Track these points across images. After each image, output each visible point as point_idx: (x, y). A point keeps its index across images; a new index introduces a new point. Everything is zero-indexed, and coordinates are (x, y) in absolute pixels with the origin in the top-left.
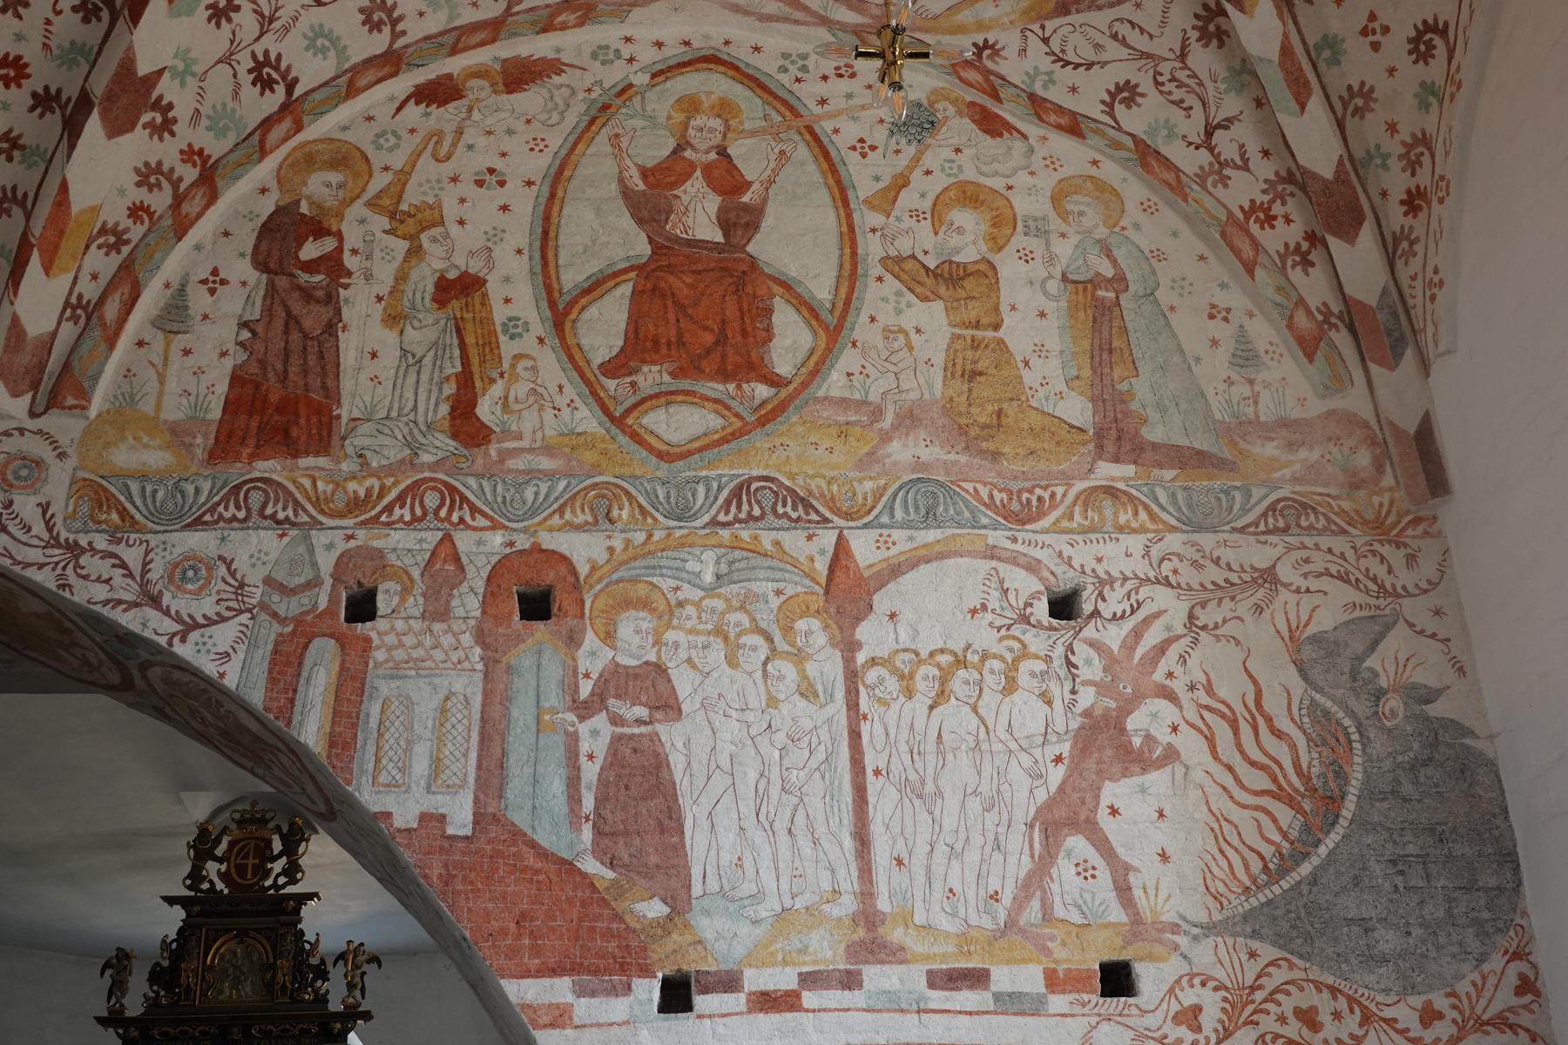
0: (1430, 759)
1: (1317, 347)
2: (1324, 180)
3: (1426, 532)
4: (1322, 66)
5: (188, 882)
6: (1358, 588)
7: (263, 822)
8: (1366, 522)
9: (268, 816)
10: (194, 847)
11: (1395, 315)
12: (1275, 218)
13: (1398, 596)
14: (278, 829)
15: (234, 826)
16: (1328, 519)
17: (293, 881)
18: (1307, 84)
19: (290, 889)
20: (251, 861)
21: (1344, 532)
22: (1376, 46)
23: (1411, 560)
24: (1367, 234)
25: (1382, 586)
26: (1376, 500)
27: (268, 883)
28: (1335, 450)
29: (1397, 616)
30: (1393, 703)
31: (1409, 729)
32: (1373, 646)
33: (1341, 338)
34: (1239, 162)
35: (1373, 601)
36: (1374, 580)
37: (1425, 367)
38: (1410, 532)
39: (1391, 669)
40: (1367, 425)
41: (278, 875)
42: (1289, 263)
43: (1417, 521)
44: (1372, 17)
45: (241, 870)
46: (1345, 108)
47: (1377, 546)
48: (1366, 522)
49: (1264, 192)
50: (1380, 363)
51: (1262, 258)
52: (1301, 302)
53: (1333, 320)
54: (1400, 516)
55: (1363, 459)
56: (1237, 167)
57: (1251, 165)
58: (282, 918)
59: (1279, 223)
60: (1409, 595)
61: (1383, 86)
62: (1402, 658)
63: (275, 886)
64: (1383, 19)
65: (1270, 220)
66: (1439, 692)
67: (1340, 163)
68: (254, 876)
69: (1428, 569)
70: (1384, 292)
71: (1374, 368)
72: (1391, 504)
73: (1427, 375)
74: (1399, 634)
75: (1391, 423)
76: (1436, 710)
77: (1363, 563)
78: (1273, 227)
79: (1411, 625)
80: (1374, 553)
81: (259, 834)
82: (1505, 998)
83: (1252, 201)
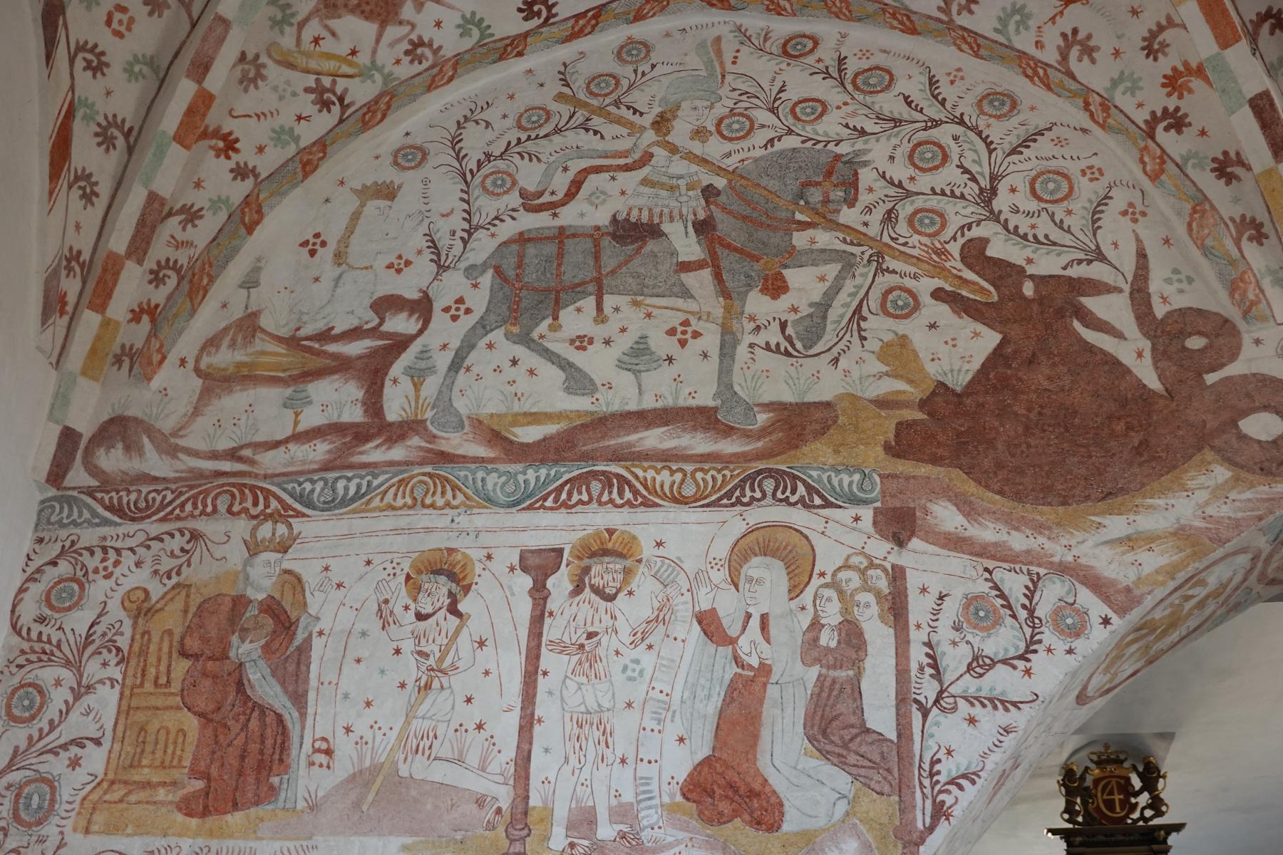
5: (1066, 816)
7: (1119, 762)
9: (1122, 757)
10: (1064, 785)
14: (1135, 768)
15: (1092, 766)
17: (1159, 814)
19: (1157, 821)
20: (1117, 797)
27: (1136, 815)
41: (1143, 809)
45: (1110, 804)
58: (1155, 847)
63: (1142, 817)
68: (1122, 809)
81: (1117, 773)
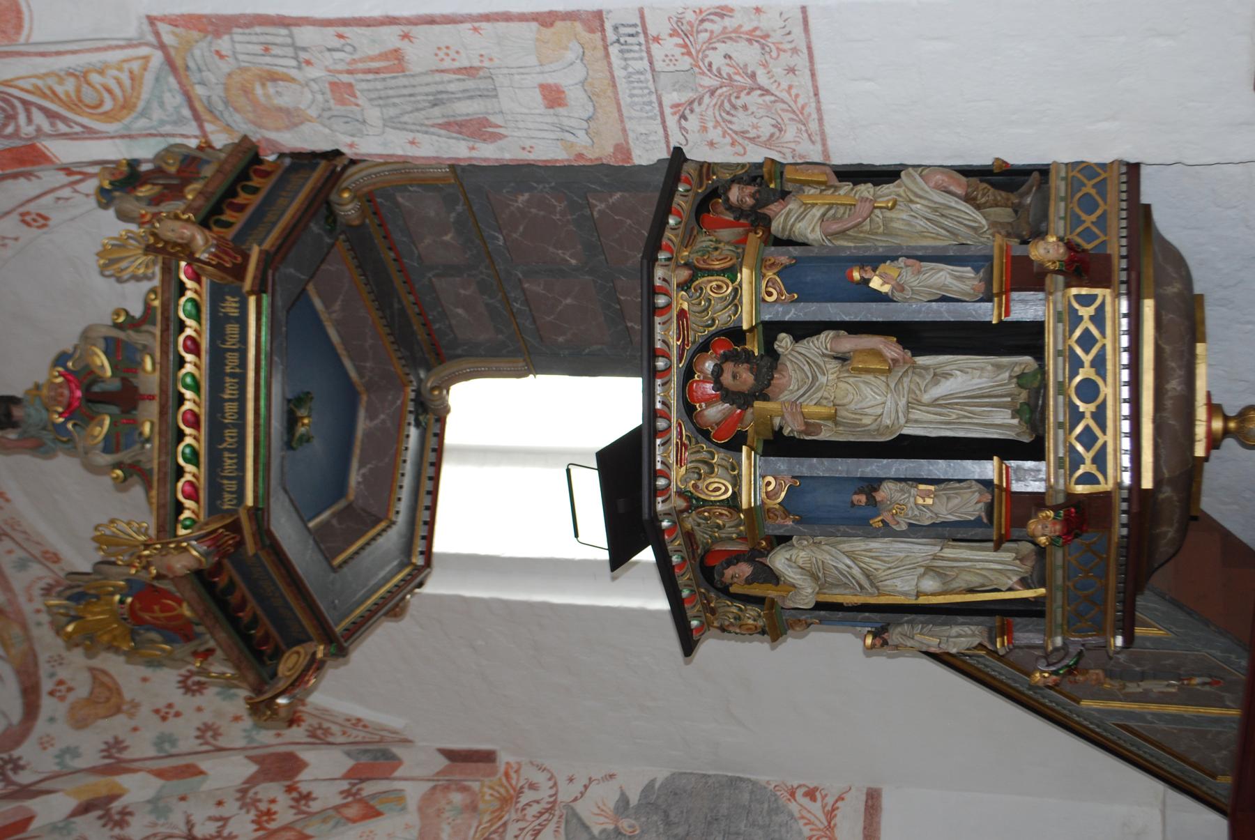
0: (665, 812)
1: (372, 808)
2: (257, 772)
3: (516, 772)
4: (174, 751)
6: (545, 826)
8: (501, 809)
11: (366, 751)
12: (269, 810)
13: (555, 802)
16: (495, 832)
18: (188, 766)
21: (505, 824)
22: (177, 714)
23: (532, 786)
24: (306, 755)
25: (547, 810)
26: (487, 797)
28: (446, 815)
29: (567, 806)
30: (625, 824)
31: (643, 819)
32: (586, 828)
33: (369, 789)
34: (220, 824)
35: (555, 819)
36: (541, 814)
37: (406, 742)
38: (514, 782)
39: (602, 819)
40: (434, 788)
42: (304, 808)
43: (507, 775)
44: (157, 711)
46: (207, 743)
47: (520, 806)
48: (501, 809)
49: (248, 812)
50: (395, 768)
51: (298, 826)
52: (337, 808)
53: (354, 790)
54: (502, 785)
55: (457, 798)
56: (223, 826)
57: (226, 815)
59: (274, 808)
60: (555, 794)
61: (207, 717)
62: (597, 811)
64: (161, 704)
65: (269, 813)
66: (623, 794)
67: (250, 758)
69: (540, 778)
70: (348, 754)
71: (397, 774)
72: (491, 788)
73: (410, 741)
74: (579, 807)
75: (438, 774)
76: (634, 799)
77: (529, 818)
78: (275, 813)
79: (576, 799)
80: (523, 809)
82: (816, 808)
83: (253, 822)
